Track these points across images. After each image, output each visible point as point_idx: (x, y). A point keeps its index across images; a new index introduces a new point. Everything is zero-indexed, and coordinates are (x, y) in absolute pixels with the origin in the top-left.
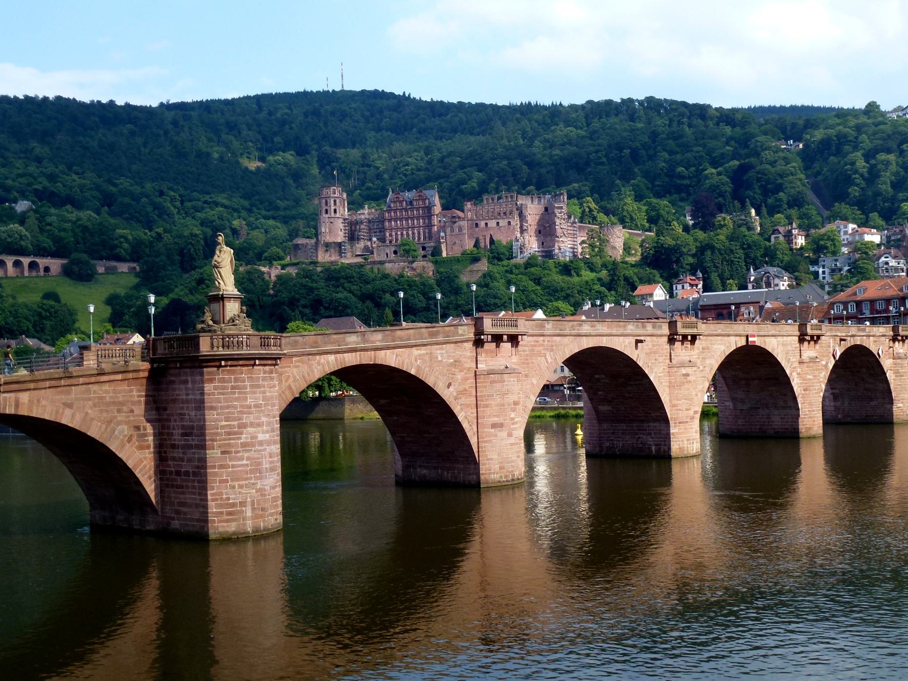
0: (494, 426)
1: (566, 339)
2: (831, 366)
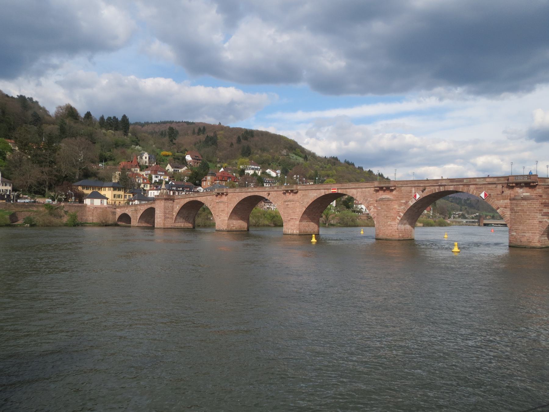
2: (411, 203)
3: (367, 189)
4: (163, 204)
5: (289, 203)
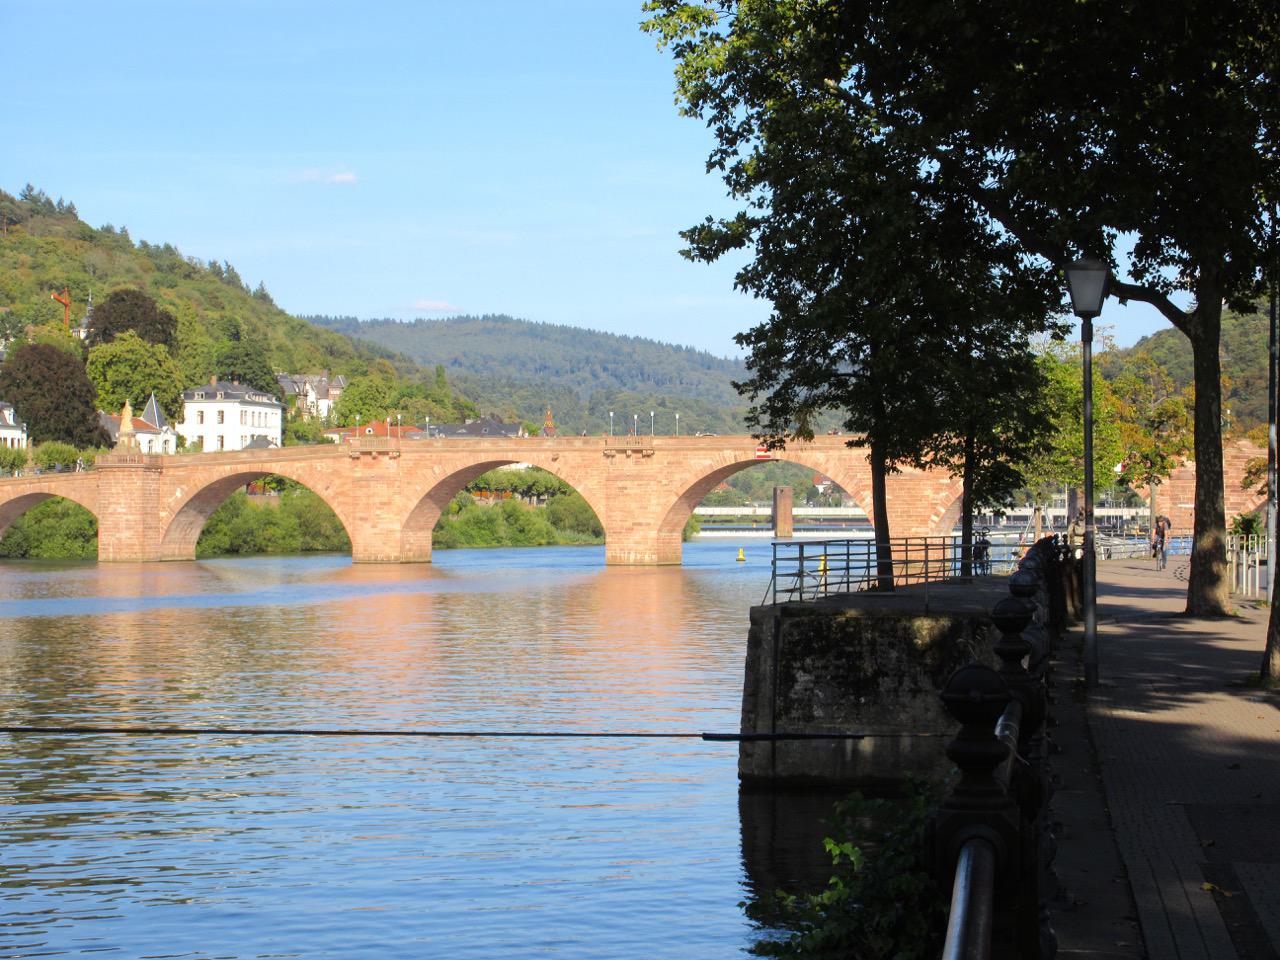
0: (362, 519)
1: (460, 455)
4: (139, 483)
5: (628, 484)
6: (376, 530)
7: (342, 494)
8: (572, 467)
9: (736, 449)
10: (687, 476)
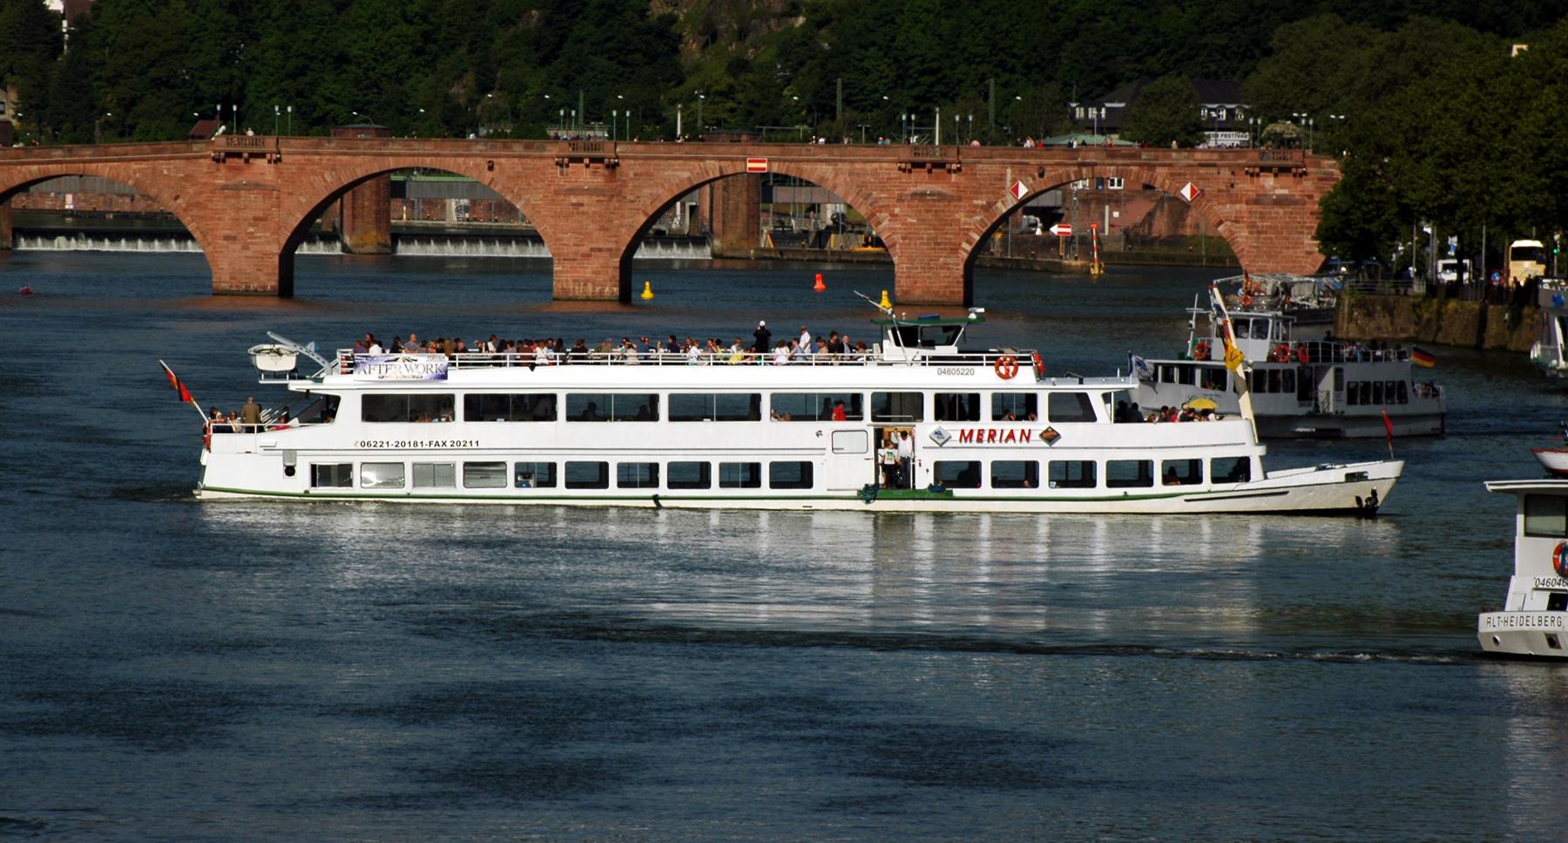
0: (226, 238)
1: (359, 159)
3: (869, 167)
5: (585, 199)
6: (248, 253)
7: (198, 205)
8: (509, 178)
9: (720, 159)
10: (661, 191)
